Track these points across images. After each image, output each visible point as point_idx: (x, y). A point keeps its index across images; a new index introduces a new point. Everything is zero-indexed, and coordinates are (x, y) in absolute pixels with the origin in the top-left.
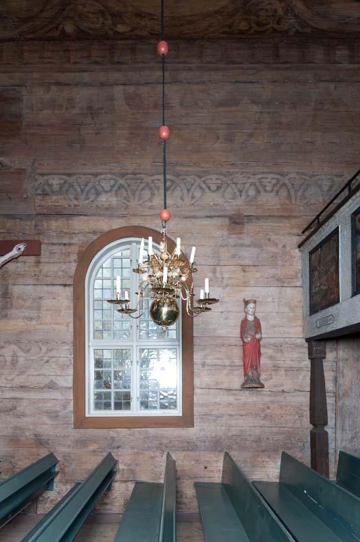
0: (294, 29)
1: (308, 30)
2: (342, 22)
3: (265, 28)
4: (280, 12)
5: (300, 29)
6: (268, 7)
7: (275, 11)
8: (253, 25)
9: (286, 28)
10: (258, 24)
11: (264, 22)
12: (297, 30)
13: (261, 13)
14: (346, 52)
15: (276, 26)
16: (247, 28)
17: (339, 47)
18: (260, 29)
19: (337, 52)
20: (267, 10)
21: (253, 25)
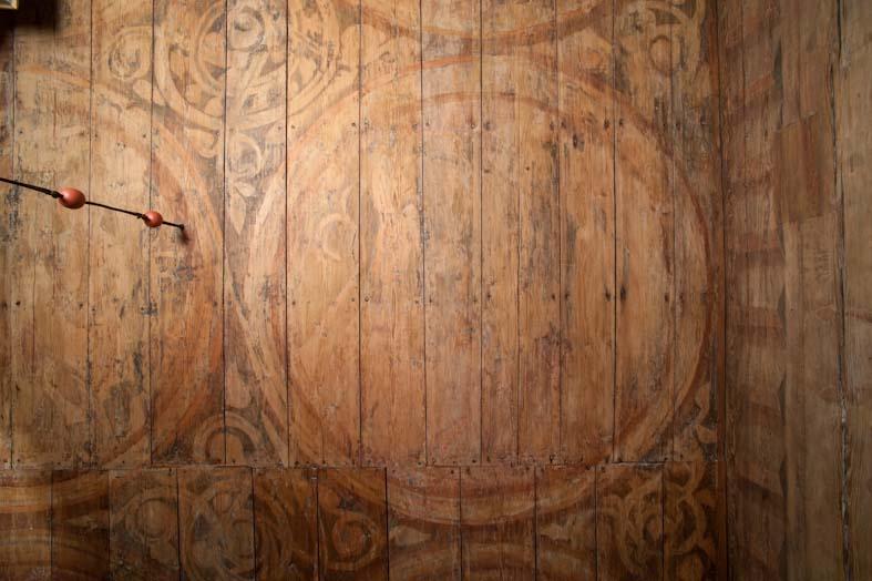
0: (702, 431)
1: (705, 391)
2: (679, 309)
3: (696, 510)
4: (654, 483)
5: (701, 416)
6: (640, 518)
7: (650, 497)
8: (689, 545)
9: (697, 456)
10: (686, 532)
11: (680, 518)
12: (706, 423)
13: (657, 534)
14: (755, 274)
15: (694, 482)
16: (697, 560)
17: (744, 299)
18: (700, 525)
19: (756, 304)
20: (647, 522)
21: (689, 545)
